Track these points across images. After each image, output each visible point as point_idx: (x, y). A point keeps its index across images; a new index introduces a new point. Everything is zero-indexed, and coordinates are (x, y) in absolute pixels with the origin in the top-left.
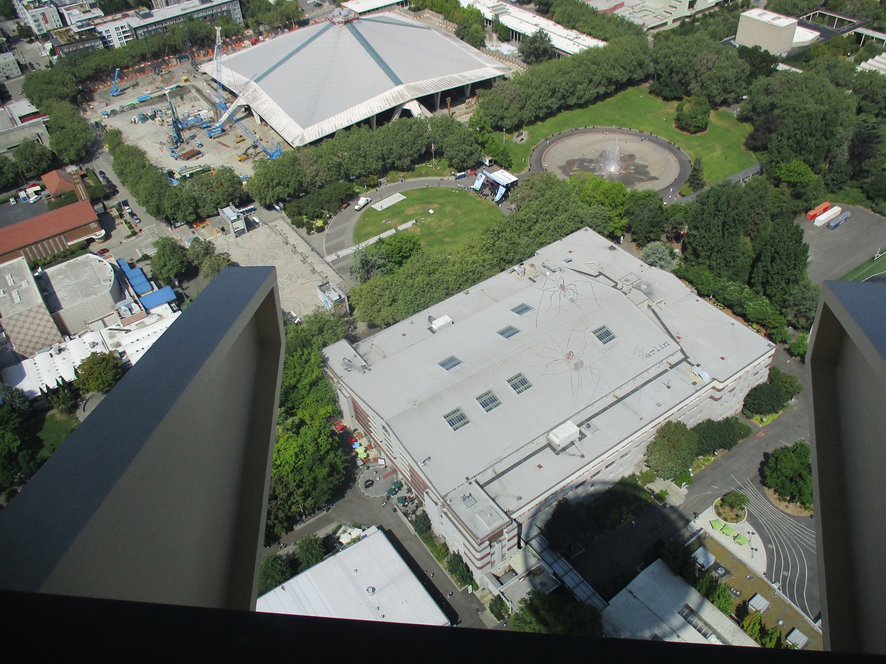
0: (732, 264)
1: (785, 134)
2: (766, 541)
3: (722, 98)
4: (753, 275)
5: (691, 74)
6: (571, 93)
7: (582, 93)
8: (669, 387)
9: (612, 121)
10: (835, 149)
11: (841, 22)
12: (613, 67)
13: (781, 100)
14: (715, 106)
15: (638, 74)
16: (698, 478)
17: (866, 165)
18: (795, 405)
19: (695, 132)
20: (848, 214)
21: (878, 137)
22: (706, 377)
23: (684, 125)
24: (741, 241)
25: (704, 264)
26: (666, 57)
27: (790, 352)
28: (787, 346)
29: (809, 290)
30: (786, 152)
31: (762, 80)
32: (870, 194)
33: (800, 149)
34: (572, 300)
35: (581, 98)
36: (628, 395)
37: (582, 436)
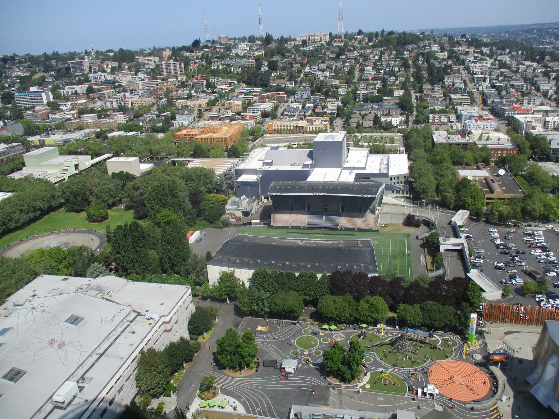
0: (150, 268)
1: (151, 198)
2: (238, 398)
3: (112, 201)
4: (163, 265)
5: (88, 193)
6: (9, 220)
7: (17, 218)
8: (133, 333)
9: (46, 231)
10: (183, 204)
11: (162, 159)
12: (34, 200)
13: (144, 189)
14: (110, 206)
15: (54, 203)
16: (180, 386)
17: (201, 206)
18: (219, 322)
19: (102, 221)
20: (204, 232)
21: (201, 192)
22: (156, 317)
23: (91, 219)
24: (149, 253)
25: (132, 272)
26: (68, 188)
27: (204, 298)
28: (200, 297)
29: (197, 257)
30: (156, 208)
31: (130, 184)
32: (210, 220)
33: (164, 205)
34: (43, 311)
35: (18, 222)
36: (107, 349)
37: (81, 389)
